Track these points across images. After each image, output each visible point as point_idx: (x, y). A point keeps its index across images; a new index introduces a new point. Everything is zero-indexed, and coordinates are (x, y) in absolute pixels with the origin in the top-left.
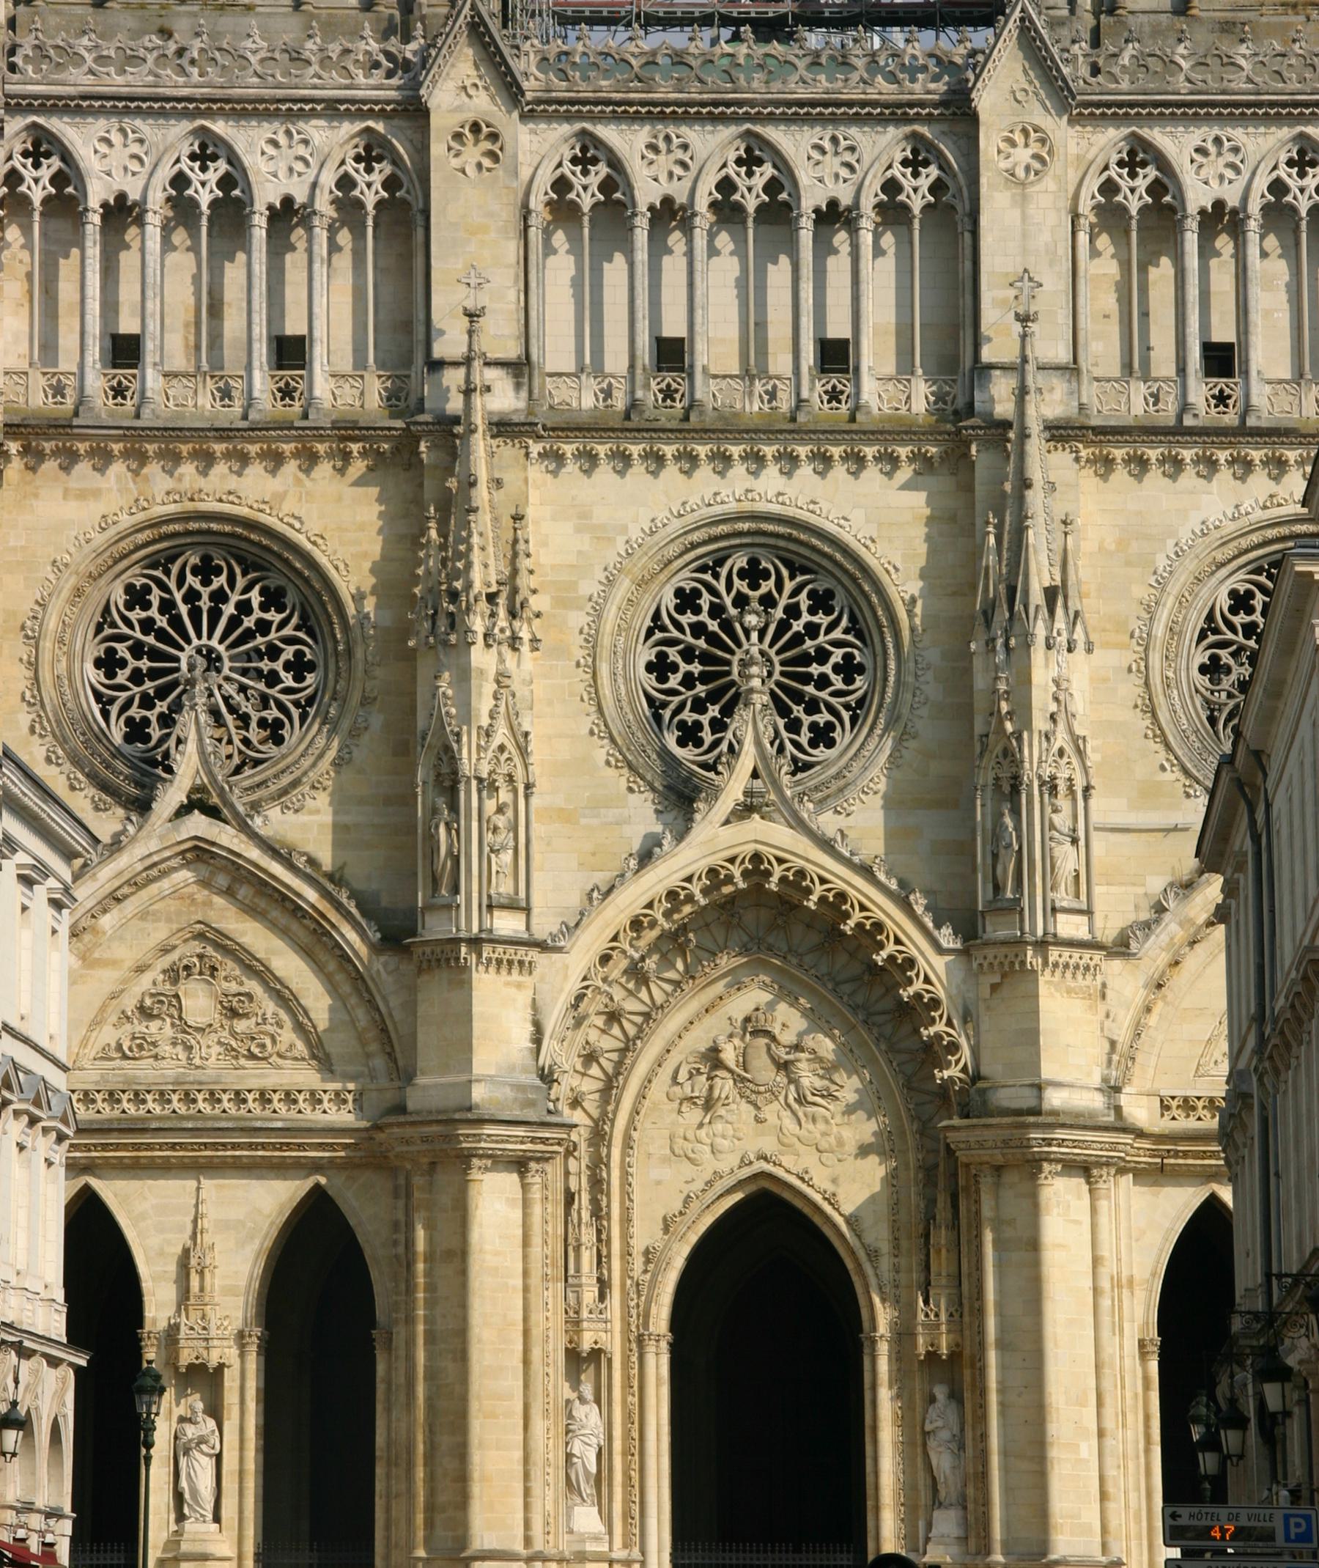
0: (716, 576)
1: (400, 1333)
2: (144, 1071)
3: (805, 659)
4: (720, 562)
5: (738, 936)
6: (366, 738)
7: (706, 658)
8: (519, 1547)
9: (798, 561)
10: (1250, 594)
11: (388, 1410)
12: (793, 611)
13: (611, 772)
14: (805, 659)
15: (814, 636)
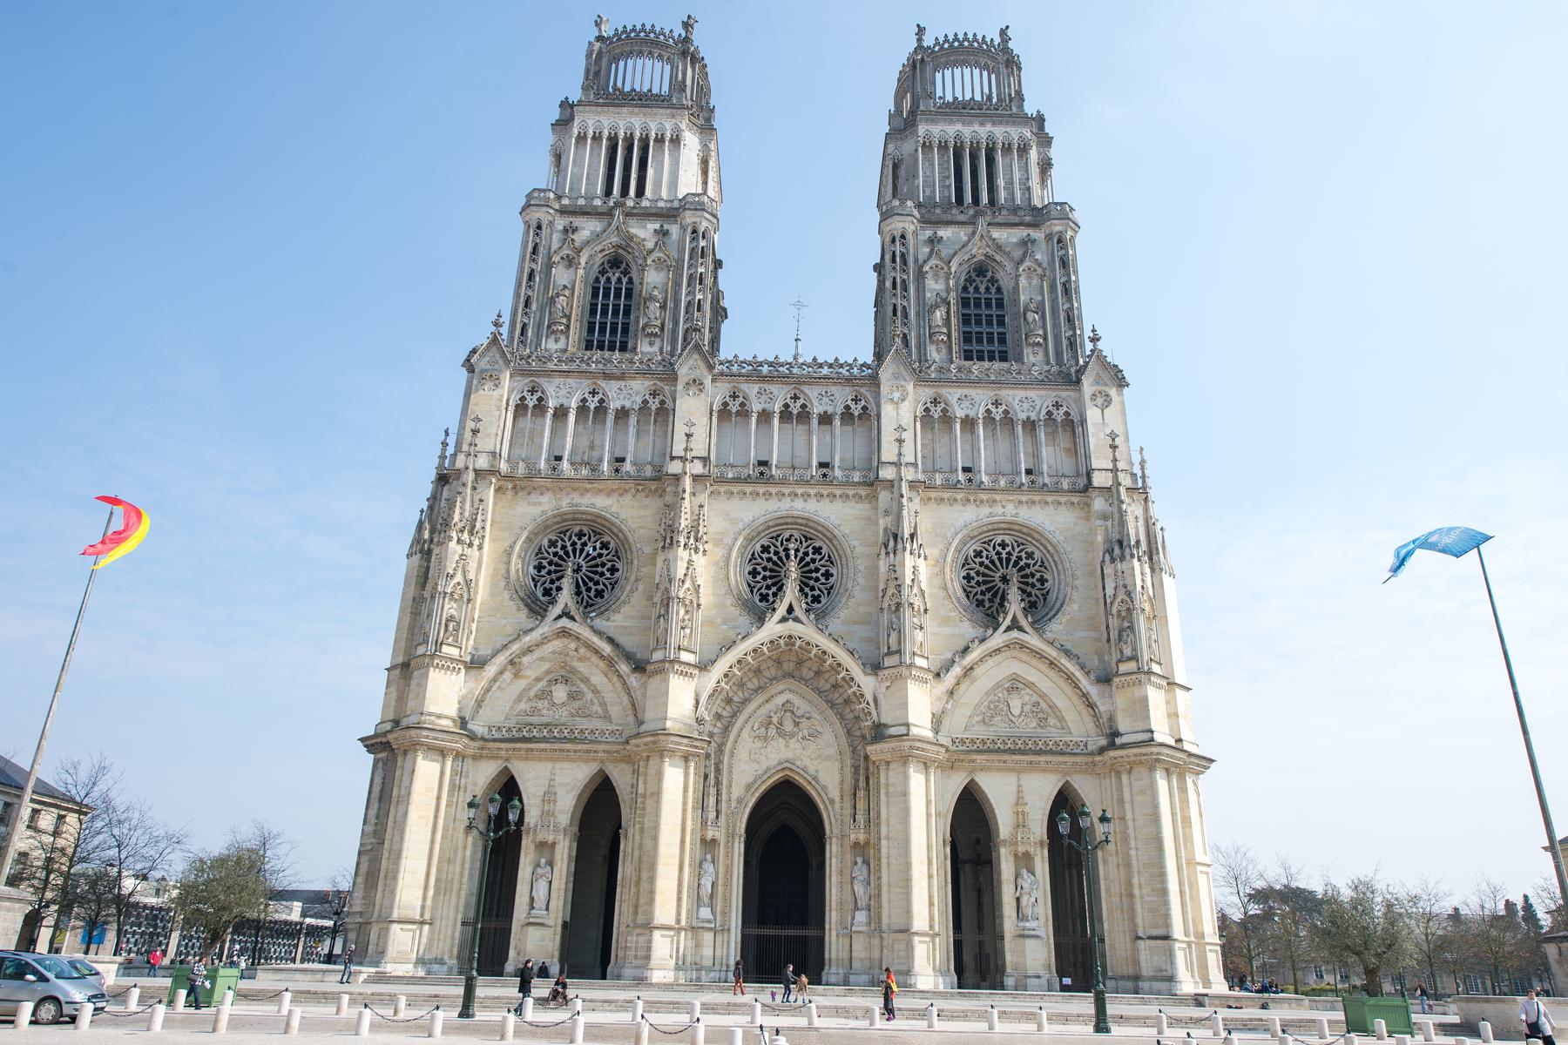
1: (631, 830)
2: (535, 720)
3: (811, 571)
8: (673, 923)
12: (806, 554)
14: (811, 571)
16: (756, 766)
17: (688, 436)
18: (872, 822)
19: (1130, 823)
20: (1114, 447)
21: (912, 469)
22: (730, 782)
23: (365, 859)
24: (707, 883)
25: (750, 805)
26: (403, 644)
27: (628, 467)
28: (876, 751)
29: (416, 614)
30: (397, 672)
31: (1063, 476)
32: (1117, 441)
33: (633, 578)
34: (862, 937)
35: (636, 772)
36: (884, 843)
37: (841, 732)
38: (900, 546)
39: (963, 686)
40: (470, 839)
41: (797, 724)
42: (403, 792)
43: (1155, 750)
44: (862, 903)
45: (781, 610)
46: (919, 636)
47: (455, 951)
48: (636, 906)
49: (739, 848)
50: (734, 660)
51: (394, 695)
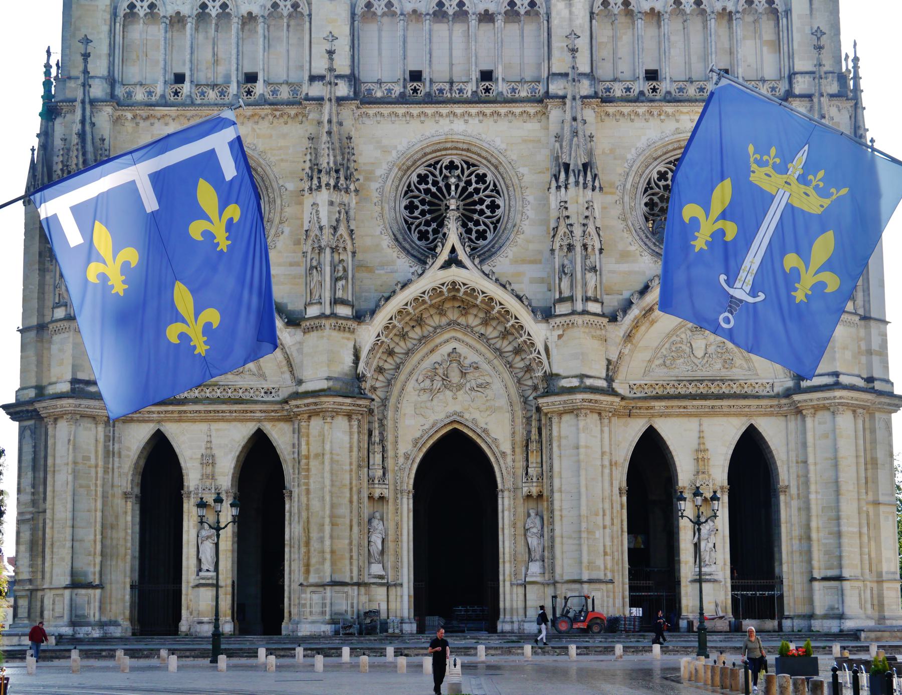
0: (435, 168)
1: (296, 492)
3: (474, 203)
4: (437, 163)
5: (444, 321)
6: (282, 237)
7: (430, 204)
8: (348, 580)
9: (471, 161)
10: (666, 173)
11: (290, 524)
12: (469, 183)
13: (390, 251)
14: (474, 203)
15: (478, 193)
16: (421, 420)
17: (331, 53)
18: (546, 474)
19: (812, 468)
20: (819, 48)
21: (586, 83)
22: (397, 437)
23: (26, 528)
24: (377, 540)
25: (418, 460)
26: (35, 304)
27: (259, 88)
28: (548, 403)
29: (43, 271)
30: (32, 334)
31: (763, 81)
32: (824, 40)
33: (277, 221)
34: (536, 587)
35: (298, 432)
36: (557, 496)
37: (511, 383)
38: (572, 179)
39: (643, 329)
40: (129, 504)
41: (463, 374)
42: (58, 461)
43: (838, 393)
44: (537, 555)
45: (444, 256)
46: (591, 278)
47: (127, 612)
48: (308, 565)
49: (407, 505)
50: (395, 311)
51: (33, 359)
